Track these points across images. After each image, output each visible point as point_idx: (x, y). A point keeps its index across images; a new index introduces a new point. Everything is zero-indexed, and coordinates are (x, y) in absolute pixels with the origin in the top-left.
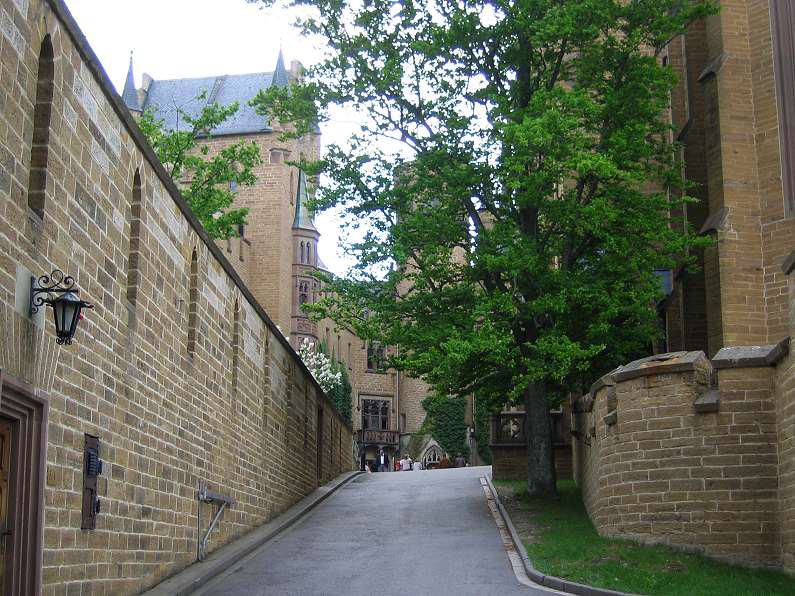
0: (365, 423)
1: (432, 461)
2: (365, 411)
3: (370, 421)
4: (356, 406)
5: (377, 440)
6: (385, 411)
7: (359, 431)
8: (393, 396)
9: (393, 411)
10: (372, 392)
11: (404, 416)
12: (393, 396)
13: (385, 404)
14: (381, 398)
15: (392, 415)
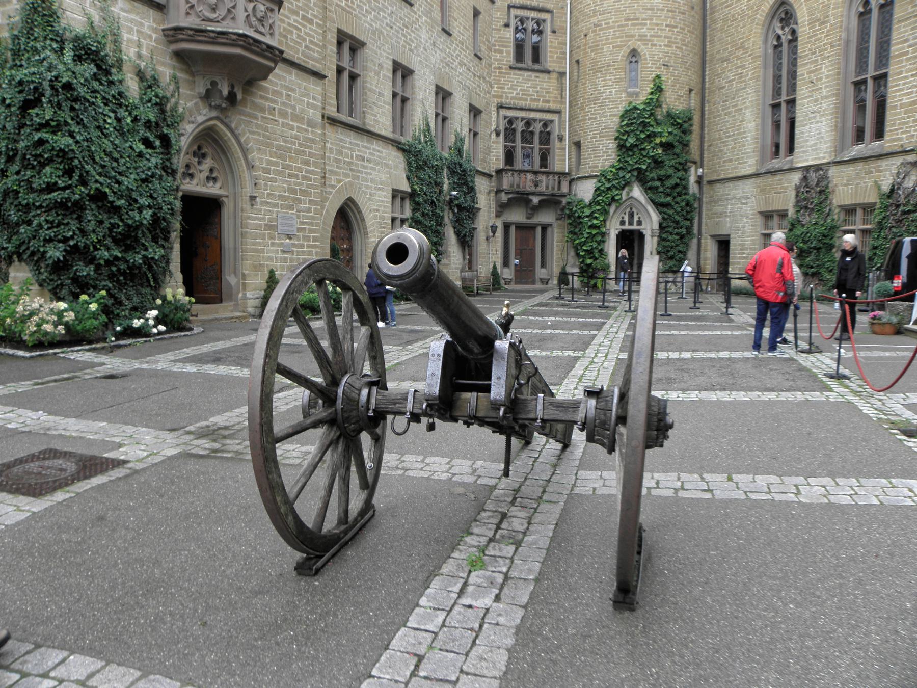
0: (509, 156)
1: (627, 227)
2: (509, 133)
3: (519, 154)
4: (494, 127)
5: (530, 187)
6: (546, 138)
7: (499, 172)
8: (558, 112)
9: (561, 139)
10: (522, 104)
11: (578, 145)
12: (558, 112)
13: (545, 125)
14: (538, 115)
15: (557, 144)
